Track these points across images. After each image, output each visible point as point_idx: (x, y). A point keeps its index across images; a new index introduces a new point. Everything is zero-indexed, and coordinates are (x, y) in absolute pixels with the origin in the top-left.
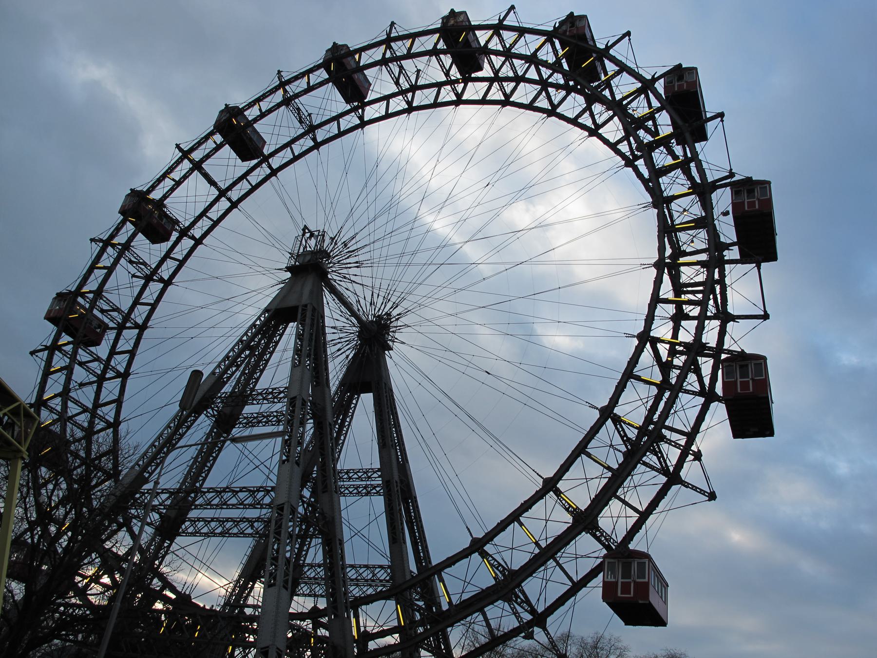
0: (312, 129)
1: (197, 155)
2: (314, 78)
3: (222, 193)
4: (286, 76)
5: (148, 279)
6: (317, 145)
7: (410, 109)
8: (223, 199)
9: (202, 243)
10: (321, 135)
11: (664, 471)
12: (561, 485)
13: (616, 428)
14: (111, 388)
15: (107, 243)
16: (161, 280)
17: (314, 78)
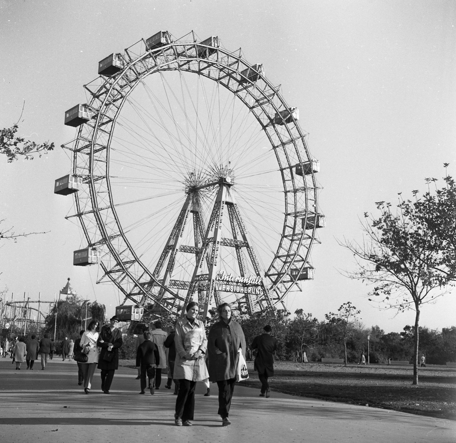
0: (295, 191)
1: (299, 142)
2: (311, 203)
3: (283, 144)
4: (318, 191)
5: (257, 101)
6: (286, 192)
7: (284, 236)
8: (280, 143)
9: (263, 129)
10: (290, 195)
11: (111, 272)
12: (121, 238)
13: (132, 261)
14: (215, 73)
15: (276, 93)
16: (253, 107)
17: (311, 203)
